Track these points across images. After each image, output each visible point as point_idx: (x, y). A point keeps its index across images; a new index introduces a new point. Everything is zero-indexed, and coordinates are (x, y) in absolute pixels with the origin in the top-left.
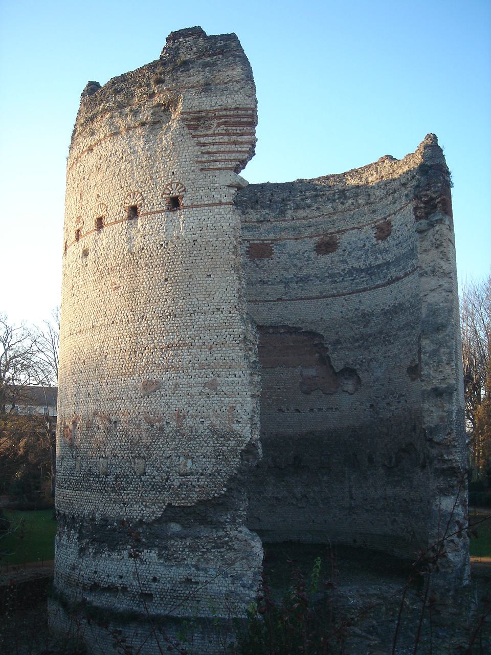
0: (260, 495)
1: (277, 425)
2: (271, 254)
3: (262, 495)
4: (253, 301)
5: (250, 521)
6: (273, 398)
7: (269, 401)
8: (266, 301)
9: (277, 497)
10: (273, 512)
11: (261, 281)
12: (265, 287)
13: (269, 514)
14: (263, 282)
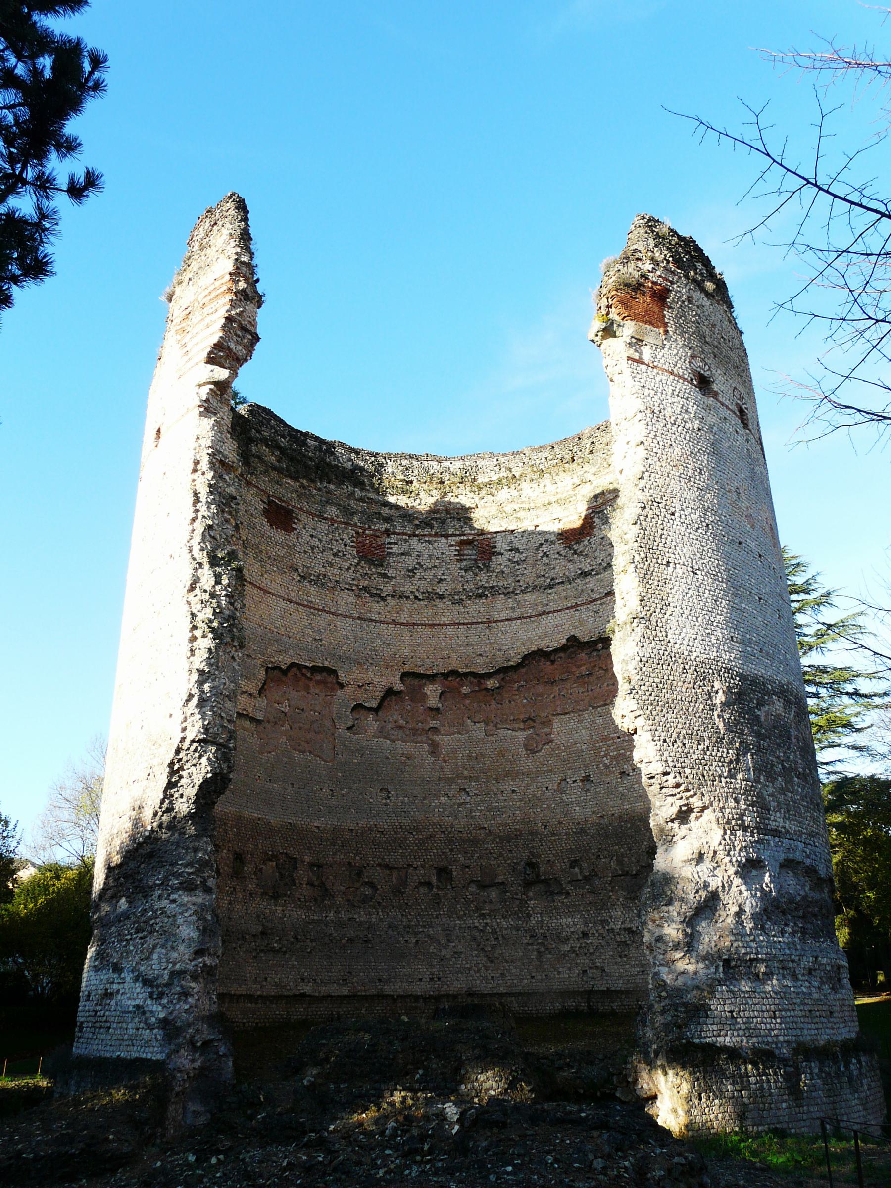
0: (604, 928)
1: (621, 799)
2: (592, 529)
3: (607, 927)
4: (572, 607)
5: (590, 975)
6: (611, 754)
7: (607, 762)
8: (591, 602)
9: (630, 928)
10: (626, 956)
11: (581, 573)
12: (587, 580)
13: (620, 960)
14: (585, 574)
